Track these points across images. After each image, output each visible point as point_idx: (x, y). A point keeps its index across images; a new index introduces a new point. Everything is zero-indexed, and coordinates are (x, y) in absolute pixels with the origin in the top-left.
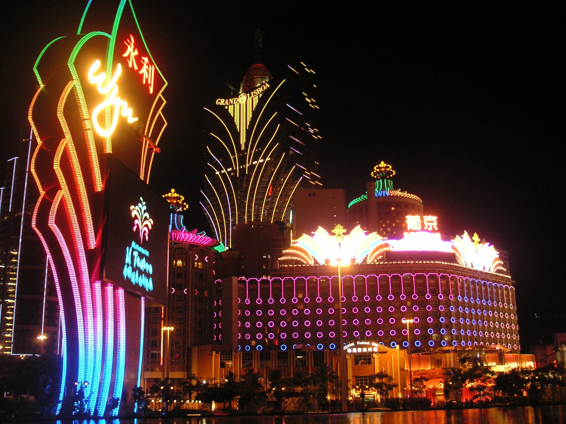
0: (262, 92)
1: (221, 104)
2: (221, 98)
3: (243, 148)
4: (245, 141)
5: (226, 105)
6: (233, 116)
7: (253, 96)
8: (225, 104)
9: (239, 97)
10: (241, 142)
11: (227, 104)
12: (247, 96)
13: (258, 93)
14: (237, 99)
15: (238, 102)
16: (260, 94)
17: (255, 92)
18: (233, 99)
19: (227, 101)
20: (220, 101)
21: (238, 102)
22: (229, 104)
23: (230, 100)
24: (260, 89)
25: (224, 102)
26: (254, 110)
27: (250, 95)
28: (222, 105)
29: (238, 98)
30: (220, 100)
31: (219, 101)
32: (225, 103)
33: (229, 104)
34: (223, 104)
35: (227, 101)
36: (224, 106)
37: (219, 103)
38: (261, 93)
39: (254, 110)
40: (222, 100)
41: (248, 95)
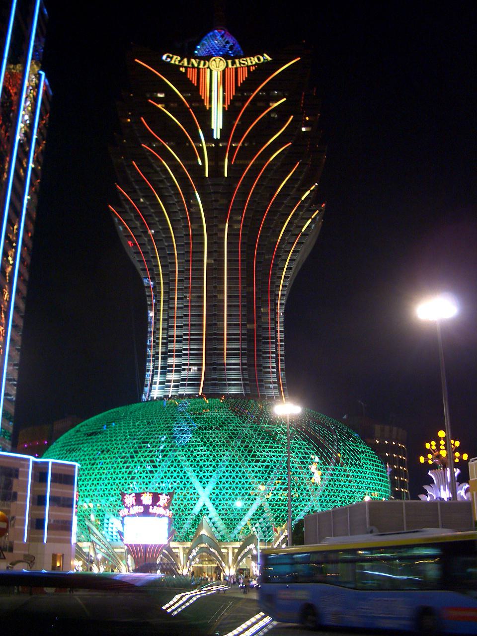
0: (256, 64)
1: (173, 62)
2: (174, 54)
3: (217, 135)
4: (220, 126)
5: (183, 66)
6: (196, 85)
7: (238, 65)
8: (181, 64)
9: (211, 60)
10: (213, 126)
12: (227, 63)
13: (250, 64)
15: (208, 67)
16: (252, 66)
17: (243, 60)
18: (198, 60)
19: (185, 60)
20: (171, 58)
21: (208, 67)
22: (190, 66)
23: (193, 61)
24: (252, 58)
25: (180, 62)
26: (239, 85)
27: (233, 63)
29: (209, 61)
30: (171, 55)
31: (168, 57)
32: (182, 62)
34: (177, 63)
35: (185, 60)
36: (180, 66)
37: (169, 60)
38: (254, 65)
39: (239, 85)
40: (175, 57)
41: (230, 62)
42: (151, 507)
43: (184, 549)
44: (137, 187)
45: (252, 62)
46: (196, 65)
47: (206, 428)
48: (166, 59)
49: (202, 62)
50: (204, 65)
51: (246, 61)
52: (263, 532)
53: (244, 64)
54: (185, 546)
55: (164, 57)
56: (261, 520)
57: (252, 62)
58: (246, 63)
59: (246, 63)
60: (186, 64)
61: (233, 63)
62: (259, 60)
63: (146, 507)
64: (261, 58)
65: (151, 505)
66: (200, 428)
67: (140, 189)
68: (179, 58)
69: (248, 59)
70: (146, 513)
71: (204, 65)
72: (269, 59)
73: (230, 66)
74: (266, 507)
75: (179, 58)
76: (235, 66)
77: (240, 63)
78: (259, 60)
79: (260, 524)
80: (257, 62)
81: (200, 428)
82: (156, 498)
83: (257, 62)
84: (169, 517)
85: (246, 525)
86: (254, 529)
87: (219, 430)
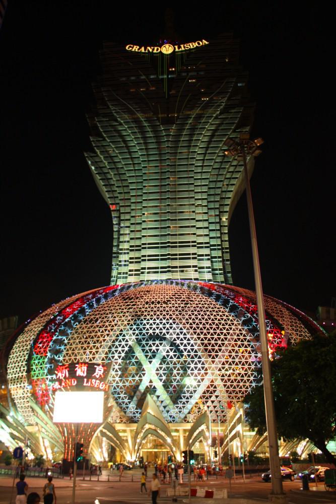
1: (133, 50)
8: (139, 51)
11: (143, 51)
14: (159, 48)
18: (152, 48)
19: (143, 48)
20: (133, 47)
23: (149, 48)
24: (194, 43)
25: (139, 49)
27: (179, 47)
28: (135, 51)
30: (132, 46)
33: (147, 51)
34: (137, 50)
35: (143, 48)
37: (131, 49)
40: (135, 47)
41: (176, 47)
42: (85, 380)
43: (131, 431)
44: (105, 136)
45: (193, 46)
46: (151, 50)
47: (153, 303)
48: (128, 48)
49: (156, 48)
50: (157, 50)
51: (189, 45)
52: (217, 412)
53: (188, 47)
54: (132, 428)
55: (127, 48)
56: (213, 398)
57: (193, 46)
58: (189, 47)
59: (189, 47)
60: (143, 51)
61: (179, 47)
62: (199, 44)
63: (80, 379)
64: (201, 43)
65: (86, 377)
66: (147, 303)
67: (107, 137)
68: (138, 47)
69: (191, 44)
70: (80, 387)
71: (157, 50)
72: (207, 43)
73: (177, 50)
74: (219, 383)
75: (138, 47)
76: (180, 50)
77: (184, 47)
78: (199, 44)
79: (213, 402)
80: (197, 45)
81: (147, 303)
82: (91, 368)
83: (197, 45)
84: (104, 390)
85: (197, 403)
86: (206, 408)
87: (167, 304)
